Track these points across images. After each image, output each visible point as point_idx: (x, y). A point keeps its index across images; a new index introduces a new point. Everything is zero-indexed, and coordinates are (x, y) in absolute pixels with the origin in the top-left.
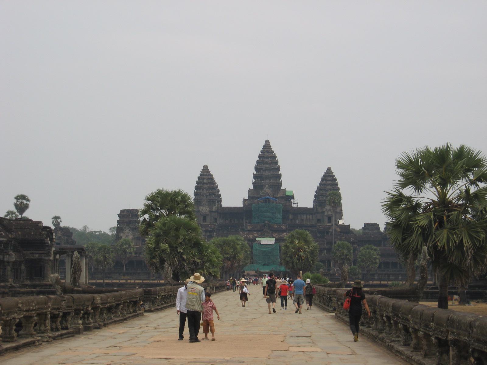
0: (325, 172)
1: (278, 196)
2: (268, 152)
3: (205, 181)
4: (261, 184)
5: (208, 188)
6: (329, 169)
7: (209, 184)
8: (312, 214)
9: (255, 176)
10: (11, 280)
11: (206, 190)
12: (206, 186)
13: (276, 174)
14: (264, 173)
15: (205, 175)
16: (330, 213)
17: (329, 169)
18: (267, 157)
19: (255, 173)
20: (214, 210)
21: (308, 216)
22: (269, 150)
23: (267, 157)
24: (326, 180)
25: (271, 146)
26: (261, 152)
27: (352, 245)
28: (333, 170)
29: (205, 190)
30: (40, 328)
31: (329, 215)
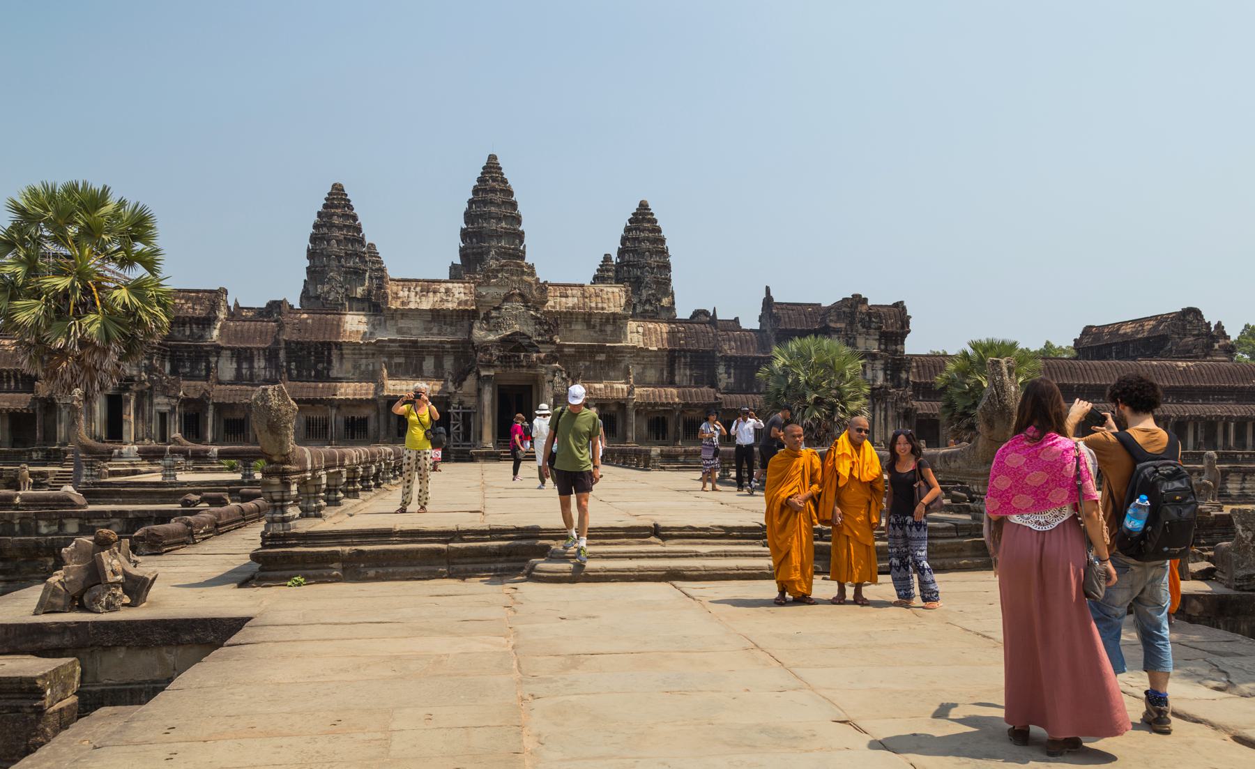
2: (494, 180)
3: (336, 221)
6: (643, 206)
9: (465, 234)
11: (339, 242)
12: (337, 233)
15: (337, 207)
17: (643, 206)
18: (493, 190)
20: (359, 296)
23: (493, 190)
24: (636, 229)
26: (480, 180)
27: (886, 345)
28: (653, 208)
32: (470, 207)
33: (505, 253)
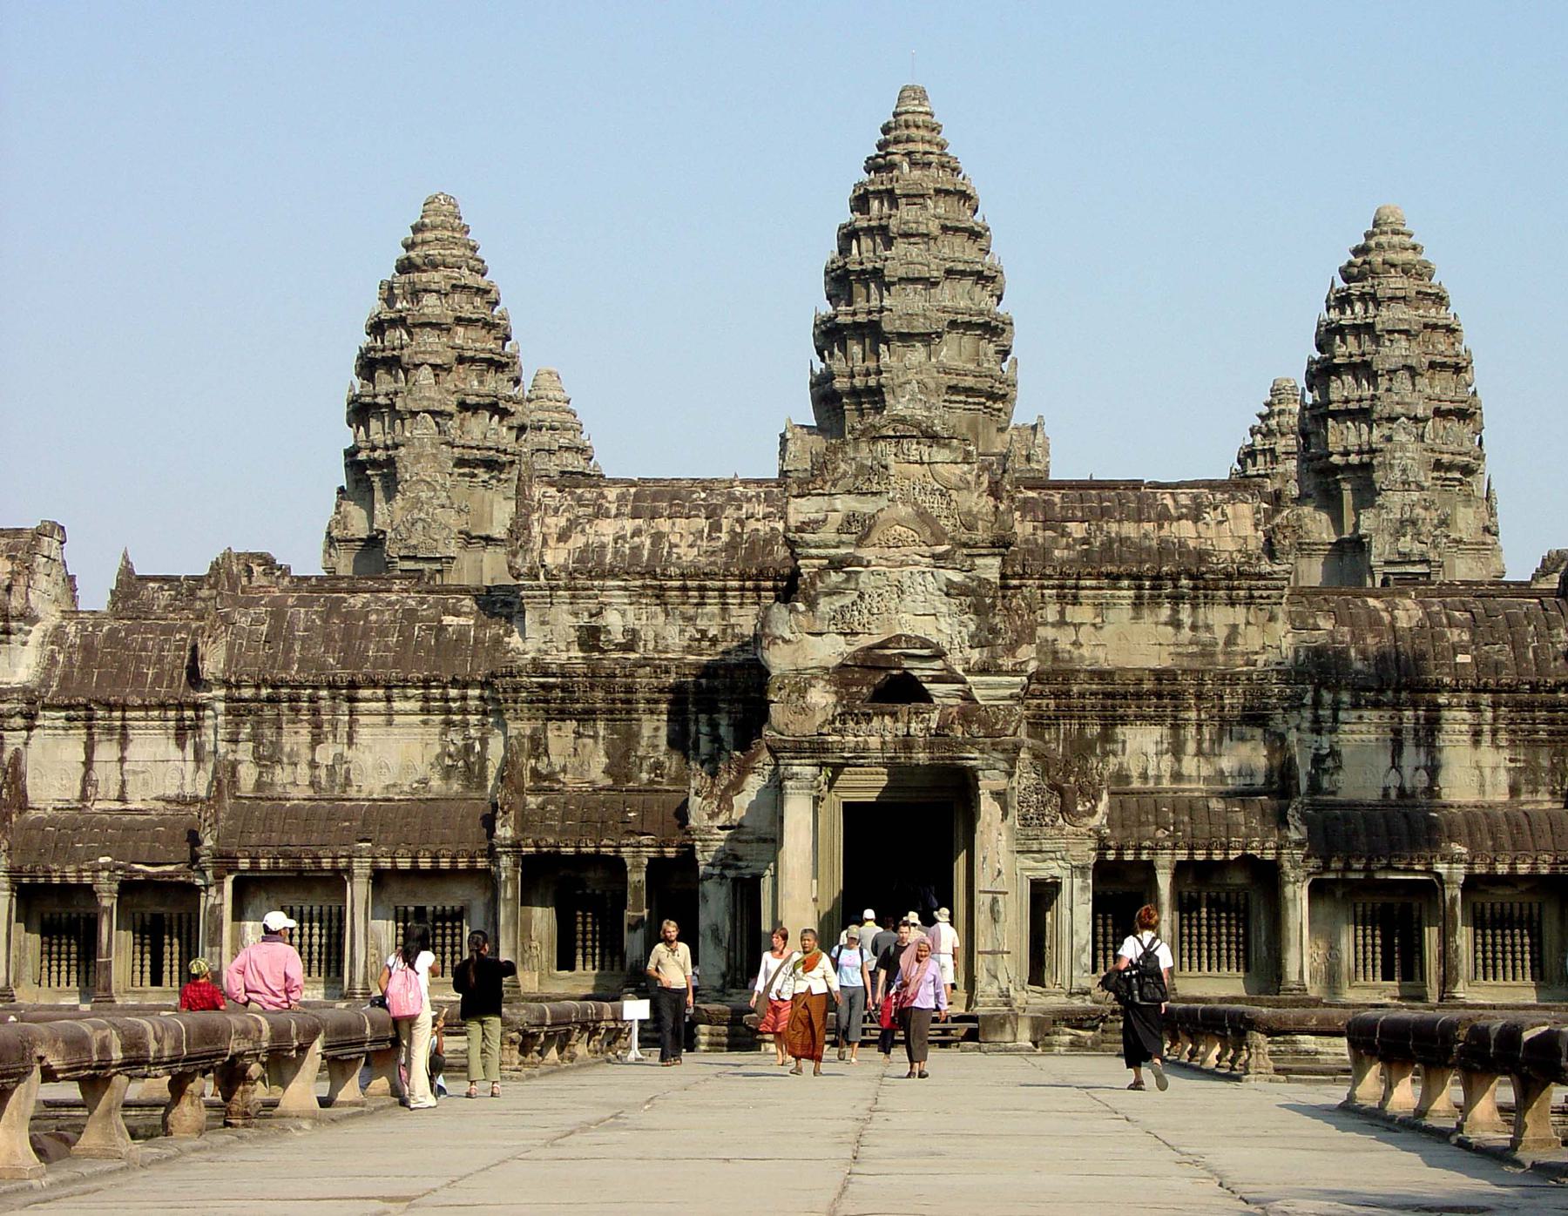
0: (1362, 241)
3: (431, 306)
4: (872, 382)
5: (448, 357)
7: (460, 330)
13: (981, 313)
14: (886, 303)
16: (1406, 544)
19: (827, 309)
22: (921, 147)
24: (1369, 298)
25: (935, 129)
29: (425, 375)
31: (1406, 559)
32: (844, 250)
33: (953, 389)
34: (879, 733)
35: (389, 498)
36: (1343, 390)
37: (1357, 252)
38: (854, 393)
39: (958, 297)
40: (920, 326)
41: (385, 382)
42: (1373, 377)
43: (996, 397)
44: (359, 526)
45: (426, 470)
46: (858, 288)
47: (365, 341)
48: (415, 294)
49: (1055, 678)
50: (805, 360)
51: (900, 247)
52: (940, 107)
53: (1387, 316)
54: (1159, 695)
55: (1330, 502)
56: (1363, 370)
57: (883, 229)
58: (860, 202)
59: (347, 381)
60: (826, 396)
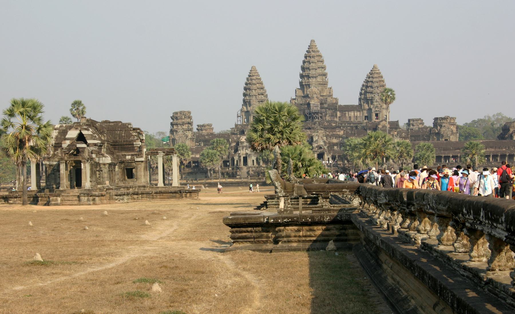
1: (325, 94)
3: (254, 82)
8: (360, 111)
10: (107, 182)
16: (376, 109)
19: (301, 72)
21: (356, 113)
24: (372, 77)
25: (316, 46)
30: (425, 227)
31: (377, 111)
34: (319, 151)
35: (250, 106)
36: (369, 89)
37: (371, 71)
38: (306, 85)
39: (319, 71)
40: (315, 76)
41: (248, 91)
42: (373, 88)
43: (325, 84)
44: (245, 109)
45: (254, 103)
46: (306, 70)
47: (245, 86)
48: (251, 80)
49: (329, 143)
50: (299, 79)
51: (312, 64)
52: (317, 43)
53: (374, 80)
54: (336, 144)
55: (368, 103)
56: (372, 87)
57: (309, 62)
58: (306, 57)
59: (243, 91)
60: (301, 84)
